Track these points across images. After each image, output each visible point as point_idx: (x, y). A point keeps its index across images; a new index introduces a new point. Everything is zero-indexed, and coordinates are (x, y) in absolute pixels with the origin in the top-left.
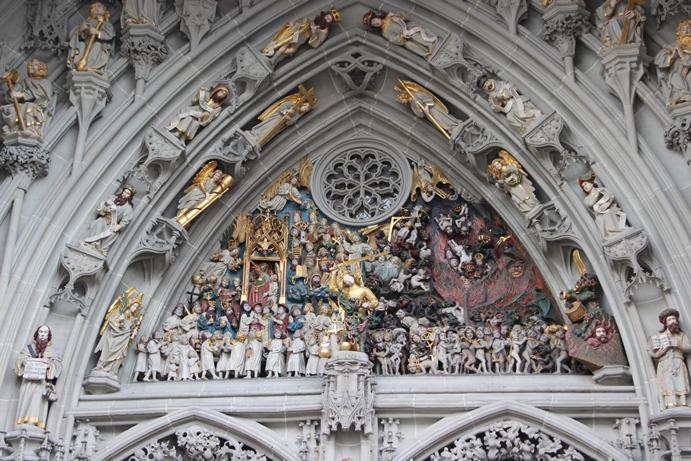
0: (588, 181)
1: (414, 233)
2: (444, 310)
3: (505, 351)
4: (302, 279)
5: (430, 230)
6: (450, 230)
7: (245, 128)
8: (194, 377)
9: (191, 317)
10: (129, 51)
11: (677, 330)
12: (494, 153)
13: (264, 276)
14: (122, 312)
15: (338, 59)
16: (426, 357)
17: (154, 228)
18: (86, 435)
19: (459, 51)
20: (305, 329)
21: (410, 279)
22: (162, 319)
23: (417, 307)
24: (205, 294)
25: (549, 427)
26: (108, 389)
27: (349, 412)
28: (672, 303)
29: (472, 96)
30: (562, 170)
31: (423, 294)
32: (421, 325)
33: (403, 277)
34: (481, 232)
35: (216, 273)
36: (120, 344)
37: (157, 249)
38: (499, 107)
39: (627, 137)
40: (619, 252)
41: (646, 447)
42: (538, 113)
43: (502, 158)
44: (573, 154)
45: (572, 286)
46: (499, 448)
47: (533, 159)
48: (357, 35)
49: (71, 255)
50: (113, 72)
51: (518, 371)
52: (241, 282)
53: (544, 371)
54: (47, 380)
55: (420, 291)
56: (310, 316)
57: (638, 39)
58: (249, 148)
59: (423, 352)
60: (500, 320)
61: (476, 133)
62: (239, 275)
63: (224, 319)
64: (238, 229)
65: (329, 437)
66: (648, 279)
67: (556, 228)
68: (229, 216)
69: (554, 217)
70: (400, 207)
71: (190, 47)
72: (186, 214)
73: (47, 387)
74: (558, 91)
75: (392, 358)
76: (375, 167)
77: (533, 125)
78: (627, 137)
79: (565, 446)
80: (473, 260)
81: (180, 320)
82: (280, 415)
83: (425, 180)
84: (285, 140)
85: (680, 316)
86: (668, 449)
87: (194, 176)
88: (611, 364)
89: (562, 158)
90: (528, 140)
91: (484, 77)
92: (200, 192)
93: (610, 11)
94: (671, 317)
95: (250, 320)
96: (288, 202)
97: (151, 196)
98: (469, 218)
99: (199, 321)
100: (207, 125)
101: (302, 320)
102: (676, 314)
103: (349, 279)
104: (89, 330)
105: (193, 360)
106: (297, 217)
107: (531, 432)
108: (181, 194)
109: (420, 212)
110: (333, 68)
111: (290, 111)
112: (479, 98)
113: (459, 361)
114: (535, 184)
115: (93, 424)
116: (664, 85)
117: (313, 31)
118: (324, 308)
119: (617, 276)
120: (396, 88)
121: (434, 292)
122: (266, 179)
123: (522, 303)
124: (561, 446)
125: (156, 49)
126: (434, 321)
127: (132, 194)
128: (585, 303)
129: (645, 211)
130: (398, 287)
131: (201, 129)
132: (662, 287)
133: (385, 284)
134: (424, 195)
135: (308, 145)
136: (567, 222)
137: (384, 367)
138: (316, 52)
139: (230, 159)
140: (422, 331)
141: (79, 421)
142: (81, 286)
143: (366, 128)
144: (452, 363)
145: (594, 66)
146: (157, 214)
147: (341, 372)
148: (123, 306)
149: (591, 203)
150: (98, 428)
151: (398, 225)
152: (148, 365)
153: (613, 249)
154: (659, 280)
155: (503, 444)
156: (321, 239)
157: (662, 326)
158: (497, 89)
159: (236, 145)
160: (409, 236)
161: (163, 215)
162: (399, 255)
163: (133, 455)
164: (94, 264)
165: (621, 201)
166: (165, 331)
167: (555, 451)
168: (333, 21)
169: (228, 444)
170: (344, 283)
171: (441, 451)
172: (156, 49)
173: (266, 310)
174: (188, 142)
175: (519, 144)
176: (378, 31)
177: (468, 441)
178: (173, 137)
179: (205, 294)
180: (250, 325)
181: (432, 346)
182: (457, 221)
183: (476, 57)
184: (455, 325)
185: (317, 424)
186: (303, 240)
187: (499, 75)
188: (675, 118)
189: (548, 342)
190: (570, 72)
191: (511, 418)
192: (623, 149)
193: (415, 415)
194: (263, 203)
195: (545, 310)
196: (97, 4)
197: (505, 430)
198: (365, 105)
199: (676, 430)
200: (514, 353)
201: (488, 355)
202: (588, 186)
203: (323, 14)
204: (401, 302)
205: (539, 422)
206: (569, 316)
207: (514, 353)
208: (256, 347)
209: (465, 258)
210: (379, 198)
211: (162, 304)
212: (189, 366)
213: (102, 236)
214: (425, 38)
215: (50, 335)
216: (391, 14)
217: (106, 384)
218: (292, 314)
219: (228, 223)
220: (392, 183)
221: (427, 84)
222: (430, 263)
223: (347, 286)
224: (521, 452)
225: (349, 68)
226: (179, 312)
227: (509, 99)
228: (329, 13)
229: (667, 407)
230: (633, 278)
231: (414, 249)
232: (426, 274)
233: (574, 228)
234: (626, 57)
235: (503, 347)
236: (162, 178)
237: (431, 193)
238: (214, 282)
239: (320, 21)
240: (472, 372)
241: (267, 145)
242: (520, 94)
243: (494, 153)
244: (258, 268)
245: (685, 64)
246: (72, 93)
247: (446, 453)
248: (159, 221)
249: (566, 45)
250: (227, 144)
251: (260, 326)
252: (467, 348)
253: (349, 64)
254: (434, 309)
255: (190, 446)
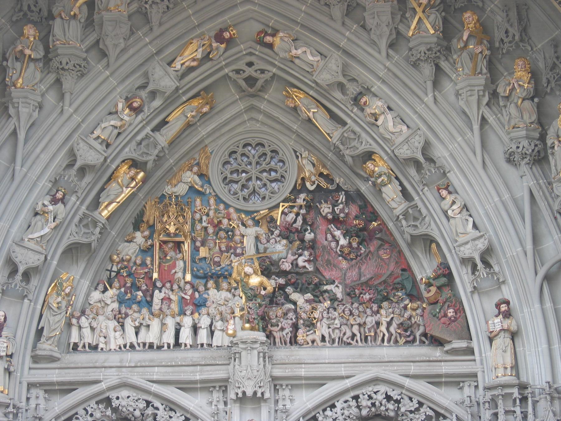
0: (445, 189)
1: (300, 219)
2: (326, 288)
3: (375, 326)
4: (205, 258)
5: (312, 214)
6: (330, 217)
7: (157, 129)
8: (120, 348)
9: (111, 292)
10: (58, 68)
11: (507, 315)
12: (369, 156)
13: (171, 254)
14: (58, 295)
15: (234, 67)
16: (312, 332)
17: (81, 220)
18: (37, 397)
19: (340, 70)
20: (208, 303)
21: (297, 259)
22: (88, 295)
23: (303, 284)
24: (122, 271)
25: (409, 390)
26: (52, 359)
27: (252, 383)
28: (507, 292)
29: (350, 108)
30: (423, 177)
31: (308, 273)
32: (307, 301)
33: (291, 258)
34: (356, 217)
35: (130, 253)
36: (59, 321)
37: (84, 240)
38: (373, 120)
39: (475, 155)
40: (467, 251)
41: (481, 404)
42: (405, 128)
43: (375, 161)
44: (432, 165)
45: (430, 273)
46: (369, 407)
47: (400, 164)
48: (250, 47)
49: (17, 249)
50: (43, 88)
51: (386, 343)
52: (152, 261)
53: (407, 342)
54: (7, 356)
55: (305, 270)
56: (213, 292)
57: (485, 71)
58: (159, 147)
59: (309, 327)
60: (371, 296)
61: (352, 136)
62: (149, 253)
63: (140, 293)
64: (148, 213)
65: (235, 401)
66: (488, 274)
67: (417, 223)
68: (141, 202)
69: (417, 214)
70: (287, 194)
71: (108, 61)
72: (106, 207)
73: (7, 361)
74: (420, 108)
75: (284, 333)
76: (265, 154)
77: (401, 139)
78: (475, 153)
79: (421, 404)
80: (350, 243)
81: (101, 295)
82: (195, 382)
83: (308, 170)
84: (187, 135)
85: (511, 303)
86: (497, 408)
87: (113, 173)
88: (459, 339)
89: (423, 168)
90: (396, 152)
91: (361, 94)
92: (118, 187)
93: (462, 45)
94: (504, 305)
95: (162, 295)
96: (190, 187)
97: (79, 195)
98: (347, 204)
99: (118, 296)
100: (124, 131)
101: (206, 296)
102: (507, 303)
103: (248, 270)
104: (34, 309)
105: (118, 334)
106: (198, 202)
107: (395, 394)
108: (102, 189)
109: (304, 200)
110: (231, 74)
111: (193, 114)
112: (355, 109)
113: (338, 335)
114: (401, 184)
115: (42, 388)
116: (503, 109)
117: (214, 48)
118: (225, 285)
119: (465, 271)
120: (284, 93)
121: (317, 270)
122: (172, 168)
123: (390, 281)
124: (417, 405)
125: (80, 66)
126: (318, 297)
127: (64, 195)
128: (439, 288)
129: (487, 214)
130: (286, 266)
131: (119, 134)
132: (498, 279)
133: (275, 263)
134: (308, 184)
135: (208, 137)
136: (427, 218)
137: (278, 340)
138: (215, 63)
139: (145, 159)
140: (308, 307)
141: (31, 386)
142: (27, 276)
143: (257, 121)
144: (333, 337)
145: (448, 87)
146: (84, 208)
147: (245, 349)
148: (59, 288)
149: (446, 208)
150: (46, 391)
151: (286, 210)
152: (81, 337)
153: (462, 249)
154: (495, 273)
155: (373, 405)
156: (220, 222)
157: (497, 311)
158: (371, 104)
159: (148, 145)
160: (295, 221)
161: (87, 209)
162: (287, 238)
163: (77, 414)
164: (37, 257)
165: (469, 205)
166: (90, 304)
167: (413, 409)
168: (231, 37)
169: (153, 406)
170: (245, 273)
171: (324, 410)
172: (80, 66)
173: (175, 287)
174: (108, 145)
175: (389, 152)
176: (270, 46)
177: (346, 402)
178: (96, 144)
179: (122, 271)
180: (162, 299)
181: (317, 322)
182: (336, 208)
183: (353, 74)
184: (334, 299)
185: (224, 389)
186: (204, 224)
187: (373, 90)
188: (512, 140)
189: (410, 318)
190: (430, 95)
191: (379, 383)
192: (471, 162)
193: (303, 382)
194: (168, 189)
195: (409, 286)
196: (29, 25)
197: (375, 393)
198: (254, 102)
199: (502, 395)
200: (383, 328)
201: (362, 330)
202: (444, 193)
203: (222, 31)
204: (290, 280)
205: (401, 386)
206: (427, 298)
207: (383, 328)
208: (170, 322)
209: (343, 242)
210: (268, 183)
211: (88, 283)
212: (115, 339)
213: (42, 233)
214: (311, 58)
215: (5, 318)
216: (281, 34)
217: (51, 356)
218: (197, 290)
219: (140, 208)
220: (280, 171)
221: (311, 93)
222: (313, 245)
223: (247, 275)
224: (387, 410)
225: (246, 75)
226: (101, 287)
227: (380, 115)
228: (226, 29)
229: (497, 377)
230: (477, 273)
231: (301, 232)
232: (310, 255)
233: (432, 222)
234: (474, 86)
235: (374, 322)
236: (88, 179)
237: (314, 183)
238: (129, 261)
239: (219, 38)
240: (349, 344)
241: (172, 143)
242: (390, 108)
243: (369, 156)
244: (166, 248)
245: (520, 96)
246: (10, 107)
247: (328, 412)
248: (84, 214)
249: (428, 70)
250: (140, 143)
251: (170, 299)
252: (346, 324)
253: (244, 71)
254: (318, 286)
255: (123, 407)
